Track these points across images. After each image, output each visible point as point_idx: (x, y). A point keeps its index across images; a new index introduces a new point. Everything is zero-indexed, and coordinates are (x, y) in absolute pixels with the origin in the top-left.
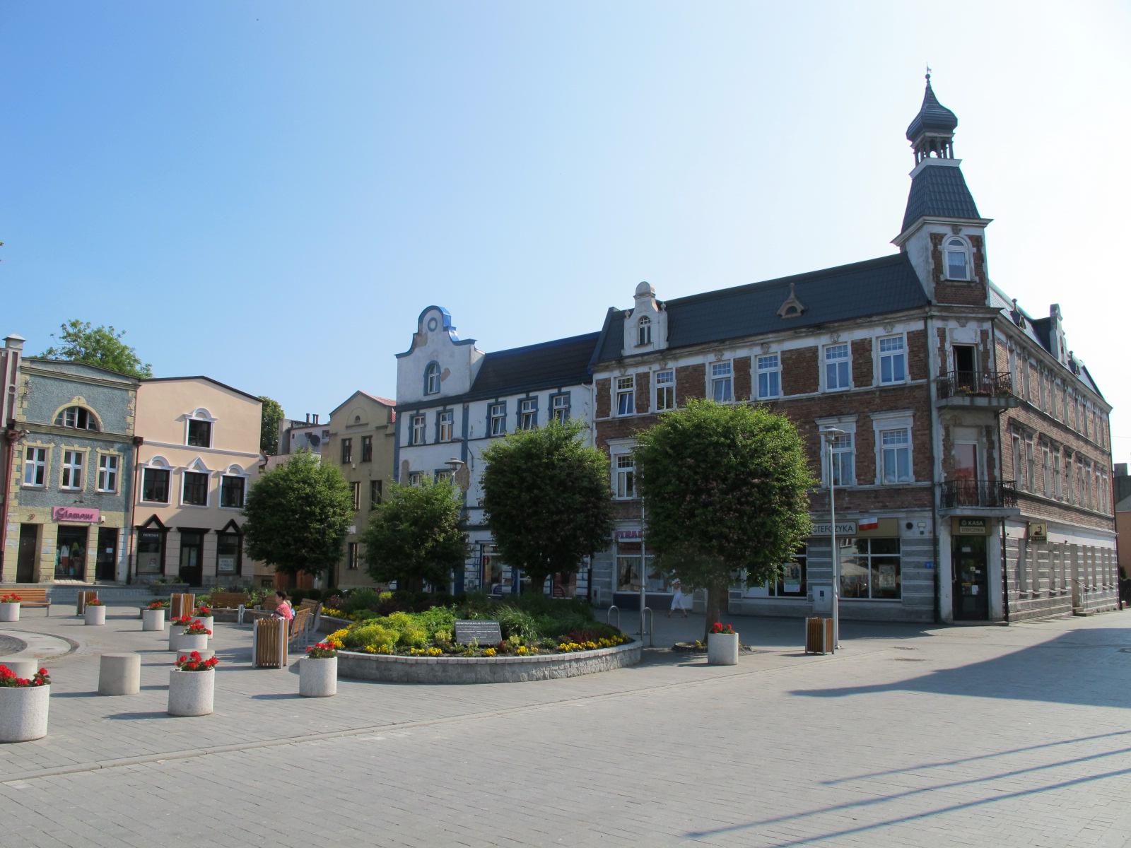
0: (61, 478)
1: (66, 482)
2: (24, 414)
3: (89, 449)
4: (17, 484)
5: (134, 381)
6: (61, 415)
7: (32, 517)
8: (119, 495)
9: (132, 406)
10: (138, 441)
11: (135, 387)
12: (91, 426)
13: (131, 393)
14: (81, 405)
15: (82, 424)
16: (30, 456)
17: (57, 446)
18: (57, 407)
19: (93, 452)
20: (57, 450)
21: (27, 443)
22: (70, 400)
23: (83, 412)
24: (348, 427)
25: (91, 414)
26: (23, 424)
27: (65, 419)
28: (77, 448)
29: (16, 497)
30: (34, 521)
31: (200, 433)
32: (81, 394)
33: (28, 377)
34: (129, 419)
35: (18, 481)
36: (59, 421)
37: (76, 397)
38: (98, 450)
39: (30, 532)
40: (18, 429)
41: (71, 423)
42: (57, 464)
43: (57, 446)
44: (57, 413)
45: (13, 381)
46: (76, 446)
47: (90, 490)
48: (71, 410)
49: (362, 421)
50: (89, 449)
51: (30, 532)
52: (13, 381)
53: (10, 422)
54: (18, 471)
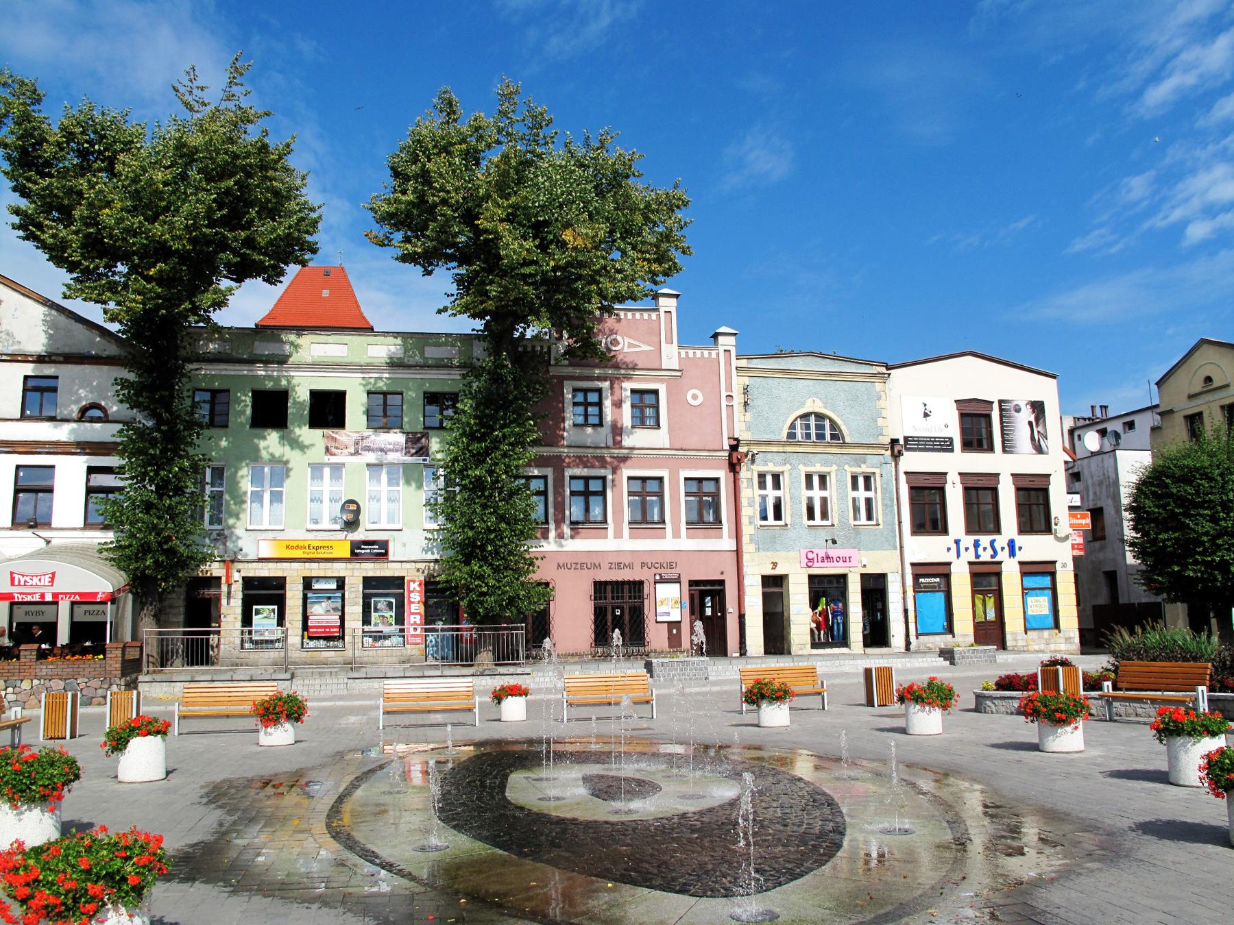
1: (811, 515)
2: (748, 429)
4: (750, 523)
5: (883, 370)
6: (793, 426)
7: (775, 565)
8: (881, 527)
9: (882, 403)
11: (885, 377)
12: (833, 437)
13: (879, 386)
14: (817, 410)
16: (762, 485)
17: (793, 468)
21: (758, 468)
22: (803, 404)
23: (820, 417)
24: (1191, 397)
25: (831, 420)
26: (750, 443)
27: (799, 432)
28: (819, 468)
29: (751, 540)
30: (778, 572)
32: (815, 394)
33: (746, 381)
34: (880, 422)
36: (791, 435)
38: (846, 467)
39: (774, 585)
40: (742, 449)
41: (808, 436)
43: (793, 468)
46: (818, 465)
47: (843, 524)
48: (806, 416)
49: (1217, 383)
50: (835, 467)
51: (774, 585)
52: (729, 387)
54: (750, 505)
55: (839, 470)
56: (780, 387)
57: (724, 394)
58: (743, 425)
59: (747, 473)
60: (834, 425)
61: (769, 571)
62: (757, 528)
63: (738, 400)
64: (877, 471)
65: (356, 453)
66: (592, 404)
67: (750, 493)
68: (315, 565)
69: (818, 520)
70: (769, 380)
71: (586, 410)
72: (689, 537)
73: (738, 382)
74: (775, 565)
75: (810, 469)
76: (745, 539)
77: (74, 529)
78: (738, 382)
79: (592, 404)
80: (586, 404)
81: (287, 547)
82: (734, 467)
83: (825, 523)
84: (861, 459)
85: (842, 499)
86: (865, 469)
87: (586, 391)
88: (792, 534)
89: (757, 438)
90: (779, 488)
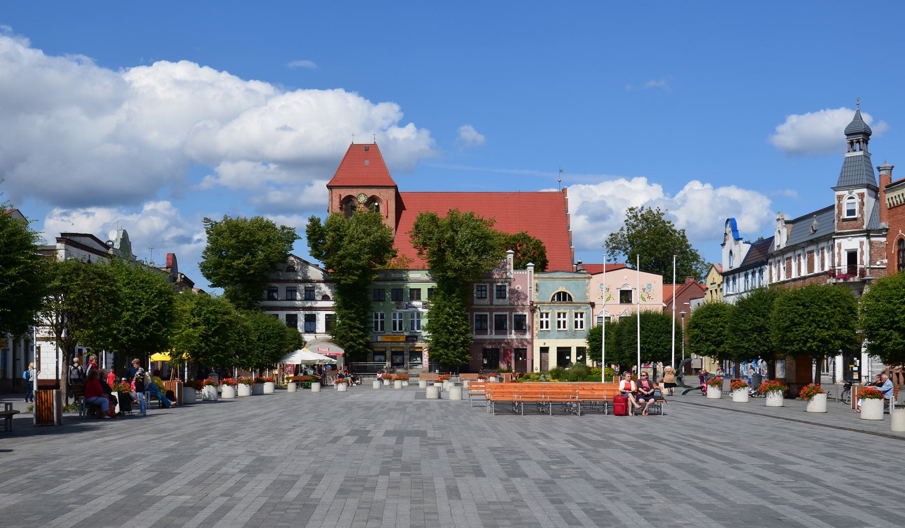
0: (557, 325)
2: (537, 298)
3: (568, 310)
5: (590, 276)
6: (554, 296)
7: (545, 344)
9: (588, 287)
10: (593, 305)
11: (589, 278)
12: (569, 300)
13: (587, 281)
14: (563, 291)
15: (564, 299)
18: (553, 291)
19: (570, 312)
20: (553, 312)
22: (558, 289)
23: (565, 294)
25: (569, 295)
28: (562, 311)
29: (537, 335)
31: (626, 296)
33: (537, 281)
34: (587, 294)
35: (537, 328)
36: (553, 299)
37: (561, 287)
38: (573, 310)
42: (552, 319)
44: (552, 296)
45: (531, 284)
47: (571, 330)
50: (568, 310)
52: (531, 284)
53: (531, 303)
55: (570, 311)
56: (549, 283)
57: (529, 286)
58: (535, 297)
59: (538, 313)
60: (569, 296)
61: (543, 346)
62: (538, 331)
63: (534, 288)
64: (585, 311)
65: (407, 308)
66: (483, 290)
67: (537, 319)
68: (395, 343)
69: (562, 328)
70: (546, 281)
71: (481, 292)
72: (496, 334)
73: (534, 282)
74: (545, 344)
75: (559, 311)
76: (535, 335)
77: (323, 333)
78: (534, 282)
79: (483, 290)
80: (481, 291)
81: (387, 338)
82: (533, 311)
83: (581, 329)
84: (579, 307)
85: (571, 321)
86: (580, 311)
87: (481, 286)
88: (551, 333)
89: (540, 301)
90: (565, 317)
